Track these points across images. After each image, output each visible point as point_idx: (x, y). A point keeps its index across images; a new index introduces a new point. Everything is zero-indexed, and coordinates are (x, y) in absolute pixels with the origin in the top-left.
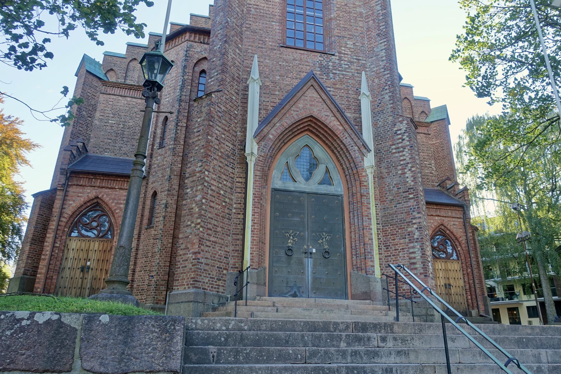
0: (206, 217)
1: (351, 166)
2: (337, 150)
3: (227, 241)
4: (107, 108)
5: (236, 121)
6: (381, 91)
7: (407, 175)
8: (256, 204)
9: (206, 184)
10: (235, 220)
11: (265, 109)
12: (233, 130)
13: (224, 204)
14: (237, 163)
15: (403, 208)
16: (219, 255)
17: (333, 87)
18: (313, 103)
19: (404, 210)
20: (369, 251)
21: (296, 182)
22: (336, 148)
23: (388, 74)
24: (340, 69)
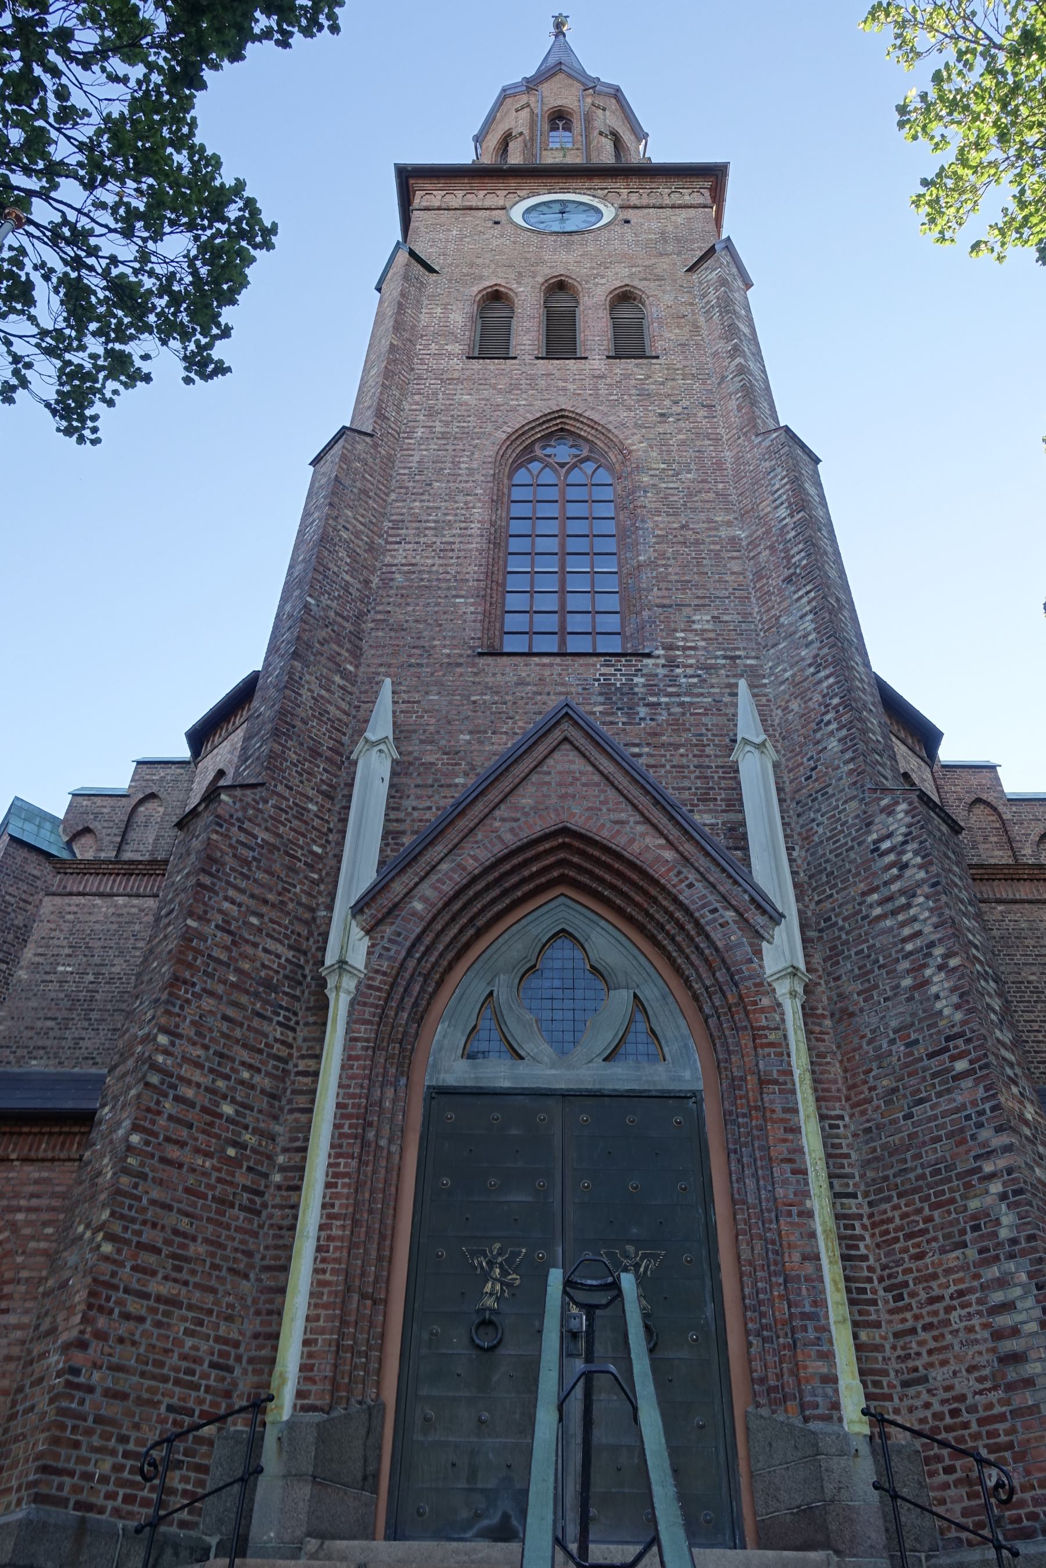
0: (139, 1199)
1: (716, 980)
2: (668, 933)
3: (231, 1299)
4: (57, 932)
5: (316, 876)
6: (815, 731)
7: (934, 989)
8: (345, 1142)
9: (154, 1079)
10: (278, 1212)
11: (416, 832)
12: (299, 903)
13: (231, 1152)
14: (308, 1009)
15: (935, 1118)
16: (184, 1357)
17: (648, 744)
18: (571, 790)
19: (943, 1126)
20: (808, 1309)
21: (522, 1058)
22: (663, 928)
23: (827, 677)
24: (670, 689)
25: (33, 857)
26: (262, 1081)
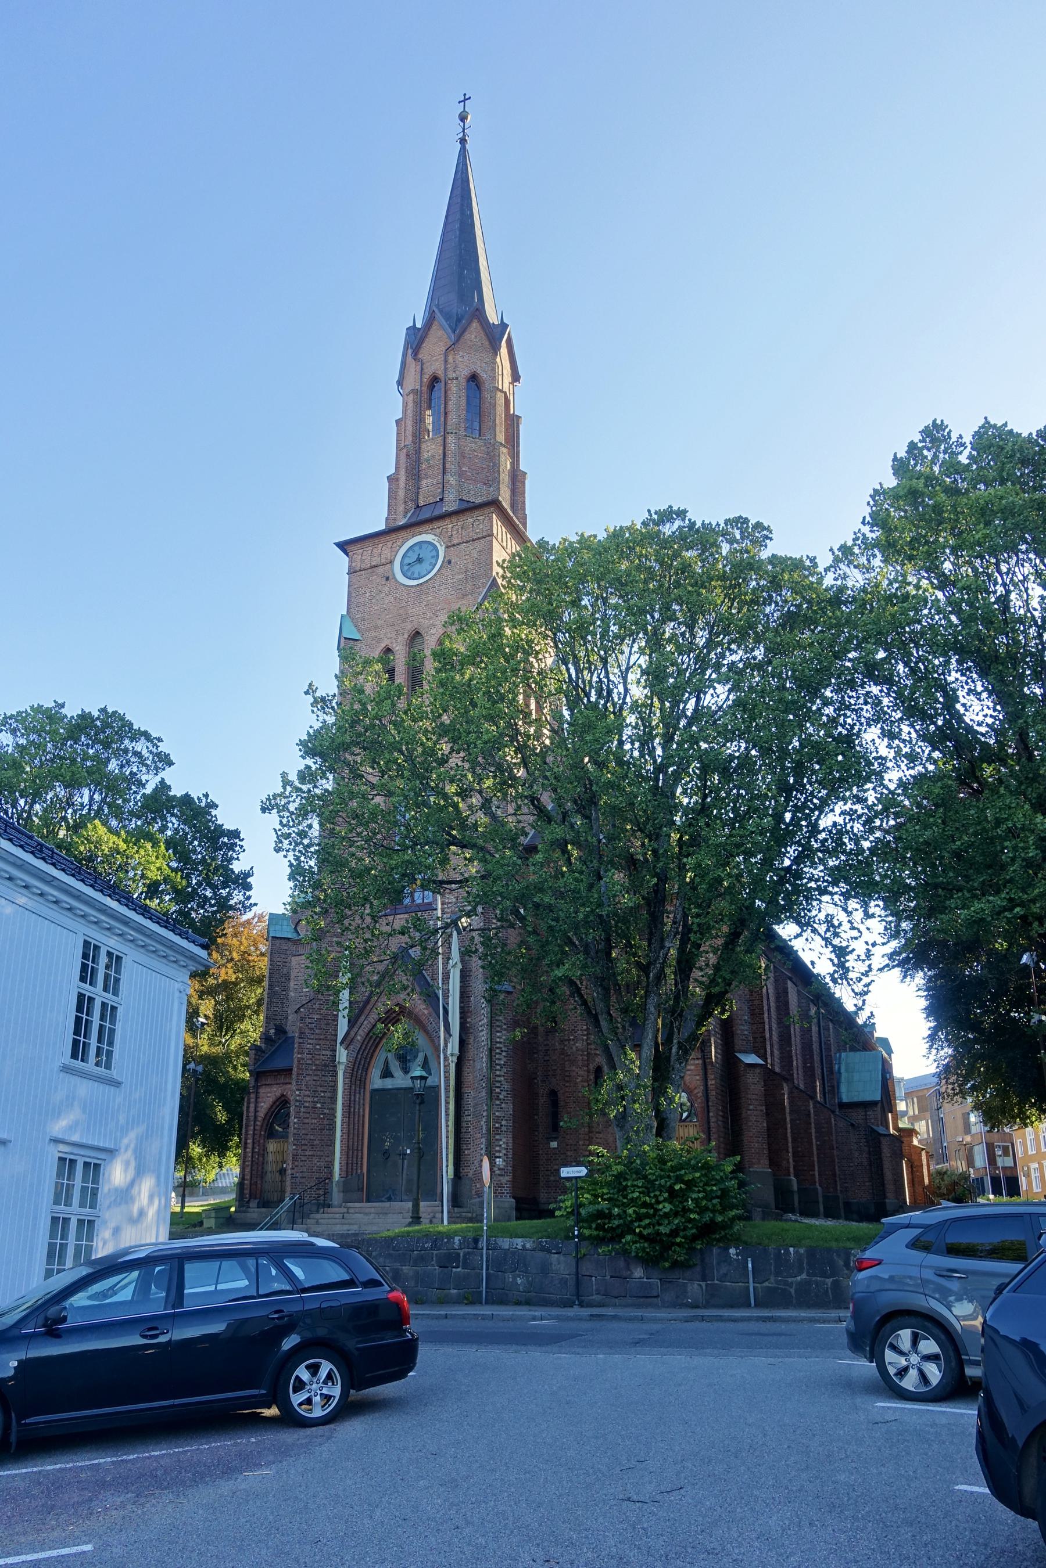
25: (283, 941)
26: (328, 1094)
